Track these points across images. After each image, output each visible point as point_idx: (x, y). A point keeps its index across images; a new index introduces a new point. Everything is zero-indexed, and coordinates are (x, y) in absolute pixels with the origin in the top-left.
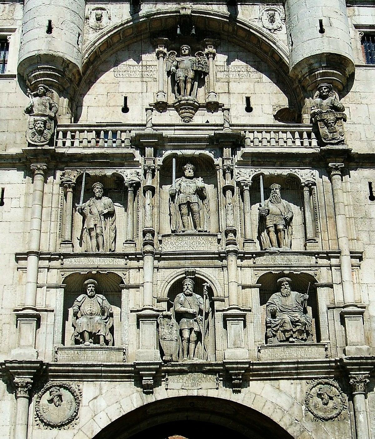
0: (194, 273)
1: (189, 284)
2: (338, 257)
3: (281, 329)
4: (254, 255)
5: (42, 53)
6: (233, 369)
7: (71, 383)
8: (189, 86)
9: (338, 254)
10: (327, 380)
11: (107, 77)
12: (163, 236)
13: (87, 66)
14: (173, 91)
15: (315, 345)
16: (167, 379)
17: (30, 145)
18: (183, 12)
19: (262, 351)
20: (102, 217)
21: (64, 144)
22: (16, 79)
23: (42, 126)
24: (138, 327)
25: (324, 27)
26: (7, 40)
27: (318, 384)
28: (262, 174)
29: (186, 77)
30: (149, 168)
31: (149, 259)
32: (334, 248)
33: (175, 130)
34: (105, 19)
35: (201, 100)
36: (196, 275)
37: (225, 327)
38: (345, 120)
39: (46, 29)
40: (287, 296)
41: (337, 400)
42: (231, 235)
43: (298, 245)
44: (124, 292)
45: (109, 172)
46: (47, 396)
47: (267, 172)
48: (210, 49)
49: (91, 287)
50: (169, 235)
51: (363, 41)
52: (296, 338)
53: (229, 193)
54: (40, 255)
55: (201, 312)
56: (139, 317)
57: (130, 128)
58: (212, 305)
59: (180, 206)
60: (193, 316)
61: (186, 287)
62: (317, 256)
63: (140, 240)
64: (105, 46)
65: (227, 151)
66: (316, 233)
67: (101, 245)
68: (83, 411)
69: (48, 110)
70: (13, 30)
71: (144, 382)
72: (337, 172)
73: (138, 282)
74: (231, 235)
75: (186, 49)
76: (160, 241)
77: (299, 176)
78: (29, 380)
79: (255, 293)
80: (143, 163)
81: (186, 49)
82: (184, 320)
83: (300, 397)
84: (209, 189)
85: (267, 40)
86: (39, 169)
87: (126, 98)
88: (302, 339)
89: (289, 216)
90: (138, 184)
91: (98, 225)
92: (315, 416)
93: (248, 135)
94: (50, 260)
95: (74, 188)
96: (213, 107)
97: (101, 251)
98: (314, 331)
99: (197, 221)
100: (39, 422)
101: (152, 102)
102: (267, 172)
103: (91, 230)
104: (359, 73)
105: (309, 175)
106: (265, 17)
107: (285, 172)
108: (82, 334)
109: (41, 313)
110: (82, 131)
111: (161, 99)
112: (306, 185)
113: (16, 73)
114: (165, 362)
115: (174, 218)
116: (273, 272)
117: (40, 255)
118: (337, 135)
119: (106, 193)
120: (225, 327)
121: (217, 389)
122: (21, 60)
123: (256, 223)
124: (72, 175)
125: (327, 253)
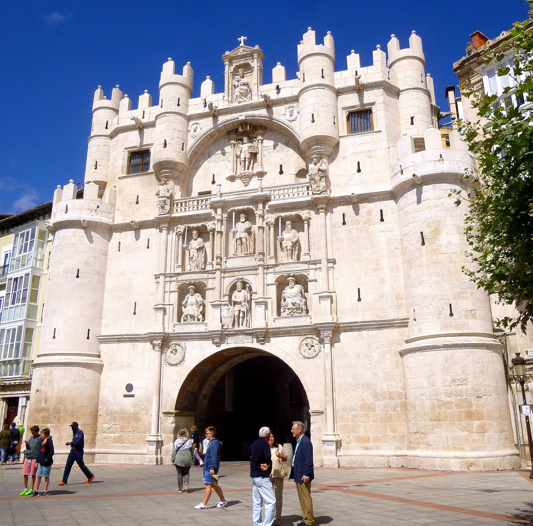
0: (242, 279)
1: (239, 284)
2: (321, 263)
3: (287, 308)
4: (274, 266)
5: (161, 161)
8: (247, 163)
9: (319, 262)
11: (206, 164)
13: (190, 161)
15: (306, 316)
16: (227, 339)
18: (240, 118)
20: (196, 251)
21: (177, 210)
27: (306, 338)
28: (281, 216)
31: (218, 272)
33: (233, 195)
35: (255, 171)
36: (244, 280)
39: (163, 145)
41: (317, 347)
44: (207, 292)
45: (200, 224)
46: (170, 350)
47: (283, 214)
48: (260, 137)
51: (348, 118)
52: (296, 312)
53: (261, 230)
54: (165, 275)
58: (251, 296)
59: (236, 240)
60: (240, 303)
61: (237, 287)
62: (308, 263)
64: (201, 146)
65: (260, 206)
70: (152, 144)
72: (322, 211)
75: (245, 139)
77: (301, 215)
78: (159, 342)
79: (274, 288)
83: (296, 346)
84: (255, 228)
85: (288, 128)
86: (164, 227)
87: (214, 175)
88: (298, 313)
90: (214, 229)
92: (304, 356)
94: (171, 277)
97: (196, 270)
100: (166, 363)
101: (228, 176)
102: (283, 214)
105: (307, 213)
106: (288, 113)
107: (293, 213)
108: (186, 316)
109: (166, 306)
112: (306, 220)
116: (284, 275)
117: (165, 275)
119: (200, 235)
121: (252, 343)
124: (181, 228)
125: (314, 261)
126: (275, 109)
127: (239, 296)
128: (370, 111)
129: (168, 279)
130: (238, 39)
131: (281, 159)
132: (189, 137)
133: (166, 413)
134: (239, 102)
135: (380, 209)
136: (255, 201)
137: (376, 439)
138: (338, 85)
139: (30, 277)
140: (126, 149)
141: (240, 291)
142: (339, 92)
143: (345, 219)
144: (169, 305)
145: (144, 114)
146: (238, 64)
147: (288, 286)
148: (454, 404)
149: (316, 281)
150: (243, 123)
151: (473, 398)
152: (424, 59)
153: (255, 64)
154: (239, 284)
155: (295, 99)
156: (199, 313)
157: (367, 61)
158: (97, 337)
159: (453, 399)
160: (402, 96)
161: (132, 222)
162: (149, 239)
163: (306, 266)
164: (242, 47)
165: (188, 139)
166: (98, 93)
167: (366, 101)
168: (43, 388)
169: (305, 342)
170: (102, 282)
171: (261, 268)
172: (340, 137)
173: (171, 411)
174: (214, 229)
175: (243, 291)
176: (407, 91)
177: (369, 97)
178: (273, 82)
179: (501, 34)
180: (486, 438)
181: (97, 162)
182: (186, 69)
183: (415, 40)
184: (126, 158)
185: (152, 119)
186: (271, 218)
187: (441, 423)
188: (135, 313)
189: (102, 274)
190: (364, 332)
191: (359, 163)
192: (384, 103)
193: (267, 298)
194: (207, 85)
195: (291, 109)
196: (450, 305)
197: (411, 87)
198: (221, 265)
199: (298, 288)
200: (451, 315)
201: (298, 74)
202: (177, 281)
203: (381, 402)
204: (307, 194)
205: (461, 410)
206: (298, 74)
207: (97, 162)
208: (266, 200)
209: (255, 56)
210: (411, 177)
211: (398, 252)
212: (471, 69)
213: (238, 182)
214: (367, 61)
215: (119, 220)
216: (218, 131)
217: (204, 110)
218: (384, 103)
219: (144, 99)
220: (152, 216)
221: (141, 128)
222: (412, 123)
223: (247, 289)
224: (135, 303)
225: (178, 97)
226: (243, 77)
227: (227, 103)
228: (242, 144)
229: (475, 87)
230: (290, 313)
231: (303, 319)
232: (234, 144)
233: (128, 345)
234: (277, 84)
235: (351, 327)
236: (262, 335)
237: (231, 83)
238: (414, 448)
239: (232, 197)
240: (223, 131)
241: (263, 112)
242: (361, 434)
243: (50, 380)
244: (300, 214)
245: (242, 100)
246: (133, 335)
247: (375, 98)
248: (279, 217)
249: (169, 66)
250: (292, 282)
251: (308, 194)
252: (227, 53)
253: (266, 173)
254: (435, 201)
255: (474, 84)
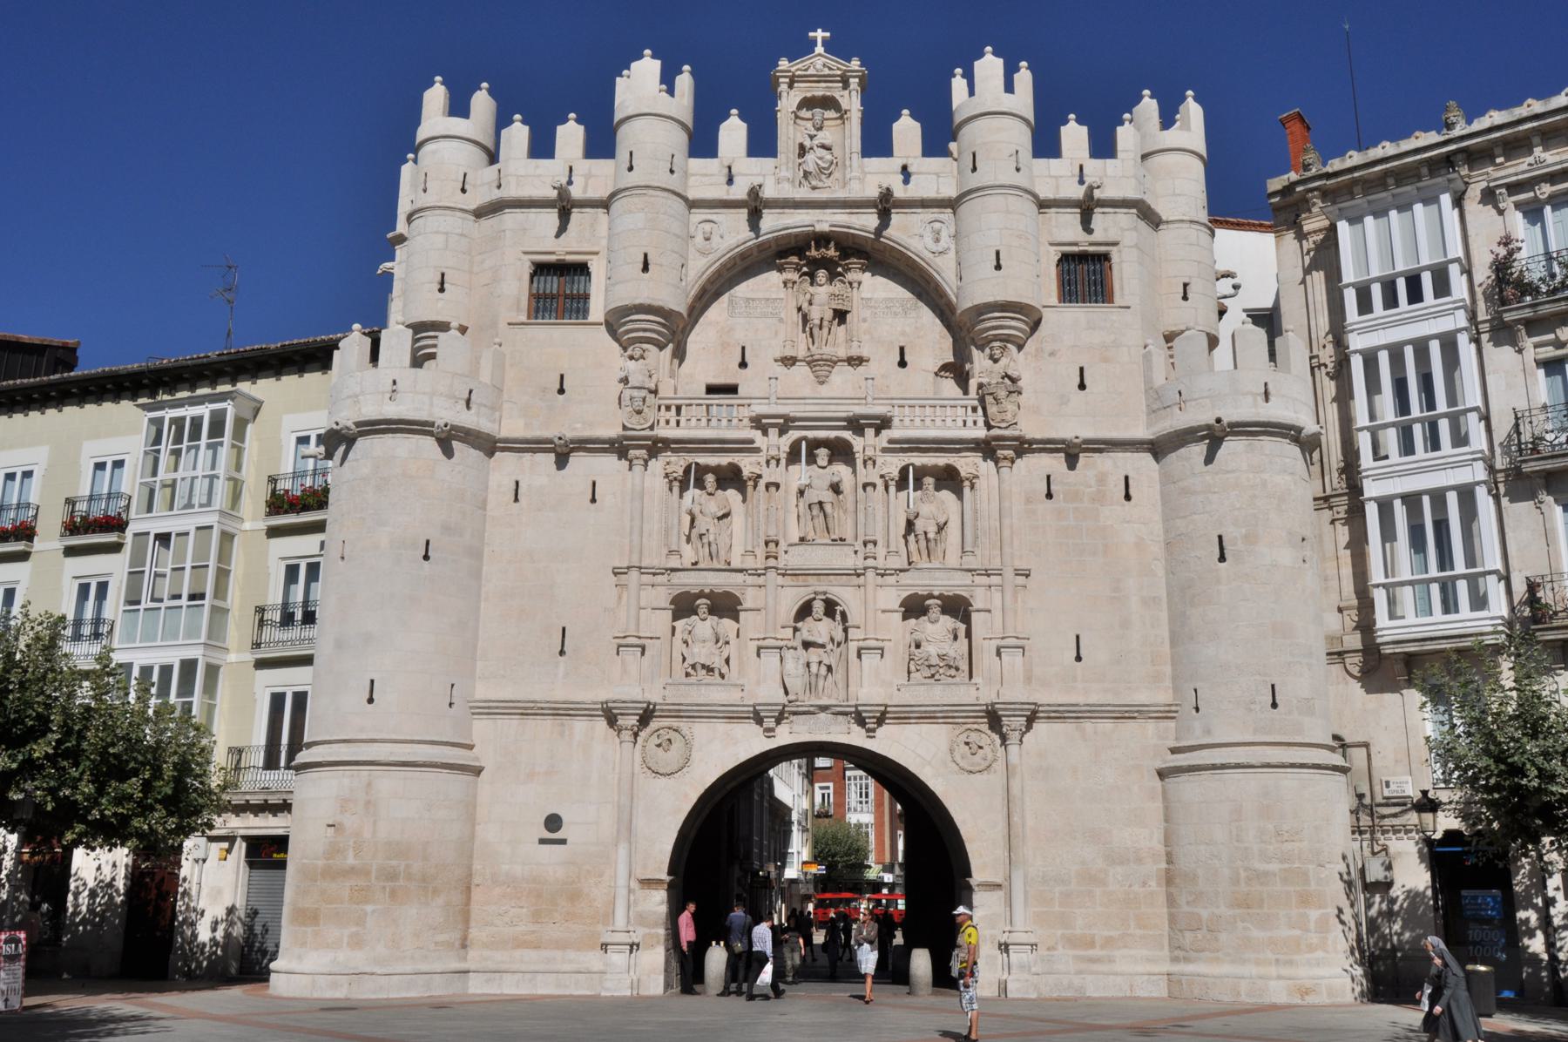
0: (825, 593)
1: (818, 607)
3: (926, 663)
6: (866, 711)
7: (682, 724)
8: (825, 330)
10: (976, 726)
12: (791, 545)
13: (691, 309)
14: (804, 331)
17: (625, 428)
19: (903, 690)
20: (716, 521)
22: (603, 328)
23: (641, 403)
24: (759, 655)
25: (1001, 262)
26: (588, 269)
28: (912, 464)
29: (822, 319)
30: (773, 458)
31: (772, 574)
32: (996, 564)
34: (715, 239)
35: (842, 353)
37: (859, 656)
38: (1020, 393)
39: (641, 266)
40: (937, 621)
41: (987, 750)
42: (870, 546)
43: (953, 559)
49: (703, 610)
50: (796, 545)
55: (832, 640)
56: (759, 649)
57: (748, 401)
58: (845, 630)
59: (810, 505)
60: (823, 646)
63: (761, 551)
66: (975, 544)
67: (714, 555)
68: (695, 755)
69: (647, 380)
71: (765, 725)
73: (759, 604)
74: (870, 546)
75: (822, 275)
76: (786, 552)
80: (765, 451)
81: (822, 275)
82: (811, 650)
83: (945, 747)
86: (637, 458)
87: (743, 348)
88: (950, 676)
89: (942, 521)
90: (760, 476)
91: (711, 531)
93: (896, 411)
94: (654, 574)
95: (680, 482)
96: (856, 361)
97: (716, 565)
98: (965, 667)
99: (830, 526)
100: (646, 769)
101: (778, 355)
103: (701, 536)
104: (1046, 314)
107: (941, 460)
108: (693, 666)
110: (691, 405)
111: (789, 353)
113: (603, 321)
114: (790, 702)
115: (802, 520)
118: (1009, 416)
120: (859, 656)
122: (608, 309)
123: (903, 524)
124: (677, 463)
125: (986, 570)
126: (896, 218)
127: (820, 628)
128: (1105, 257)
129: (647, 579)
130: (811, 34)
131: (903, 333)
132: (692, 250)
133: (648, 883)
134: (814, 188)
135: (1124, 474)
136: (856, 425)
137: (1109, 942)
138: (1045, 193)
139: (215, 534)
140: (526, 253)
141: (820, 620)
142: (1043, 205)
143: (1052, 487)
144: (651, 638)
145: (570, 176)
146: (809, 95)
147: (926, 618)
148: (1278, 878)
149: (989, 611)
150: (822, 239)
151: (1311, 867)
152: (1205, 155)
153: (852, 102)
154: (818, 607)
155: (952, 204)
156: (724, 662)
157: (1103, 146)
158: (469, 702)
159: (1274, 867)
160: (1166, 233)
161: (560, 438)
162: (594, 484)
163: (967, 579)
164: (820, 55)
165: (691, 256)
166: (436, 96)
167: (1098, 236)
168: (349, 821)
169: (965, 735)
170: (477, 574)
171: (870, 574)
172: (1044, 307)
173: (657, 877)
174: (760, 476)
175: (827, 620)
176: (1176, 225)
177: (1106, 225)
178: (895, 154)
179: (1380, 147)
180: (1329, 942)
181: (443, 275)
182: (684, 81)
183: (1193, 111)
184: (527, 277)
185: (600, 192)
186: (892, 465)
187: (1250, 911)
188: (562, 653)
189: (476, 554)
190: (1088, 725)
191: (1082, 369)
192: (1139, 248)
193: (883, 640)
194: (733, 132)
195: (937, 225)
196: (1273, 686)
197: (1185, 218)
198: (776, 558)
199: (947, 622)
200: (1274, 705)
201: (953, 146)
202: (669, 585)
203: (1119, 869)
204: (961, 424)
205: (1292, 889)
206: (953, 146)
207: (443, 275)
208: (883, 423)
209: (854, 82)
210: (1212, 422)
211: (1160, 569)
212: (1307, 201)
213: (801, 370)
214: (1103, 146)
215: (511, 427)
216: (760, 247)
217: (728, 191)
218: (1136, 246)
219: (570, 135)
220: (610, 430)
221: (565, 206)
222: (1185, 298)
223: (838, 617)
224: (564, 629)
225: (671, 151)
226: (820, 129)
227: (787, 186)
228: (812, 284)
229: (1310, 240)
230: (933, 676)
231: (963, 688)
232: (794, 283)
233: (547, 723)
234: (904, 161)
235: (1060, 714)
236: (874, 717)
237: (792, 137)
238: (1187, 960)
239: (802, 408)
240: (770, 247)
241: (867, 221)
242: (1078, 931)
243: (368, 803)
244: (954, 464)
245: (820, 184)
246: (564, 703)
247: (1119, 233)
248: (908, 465)
249: (647, 68)
250: (935, 610)
251: (975, 423)
252: (784, 64)
253: (868, 361)
254: (1251, 476)
255: (1309, 233)
